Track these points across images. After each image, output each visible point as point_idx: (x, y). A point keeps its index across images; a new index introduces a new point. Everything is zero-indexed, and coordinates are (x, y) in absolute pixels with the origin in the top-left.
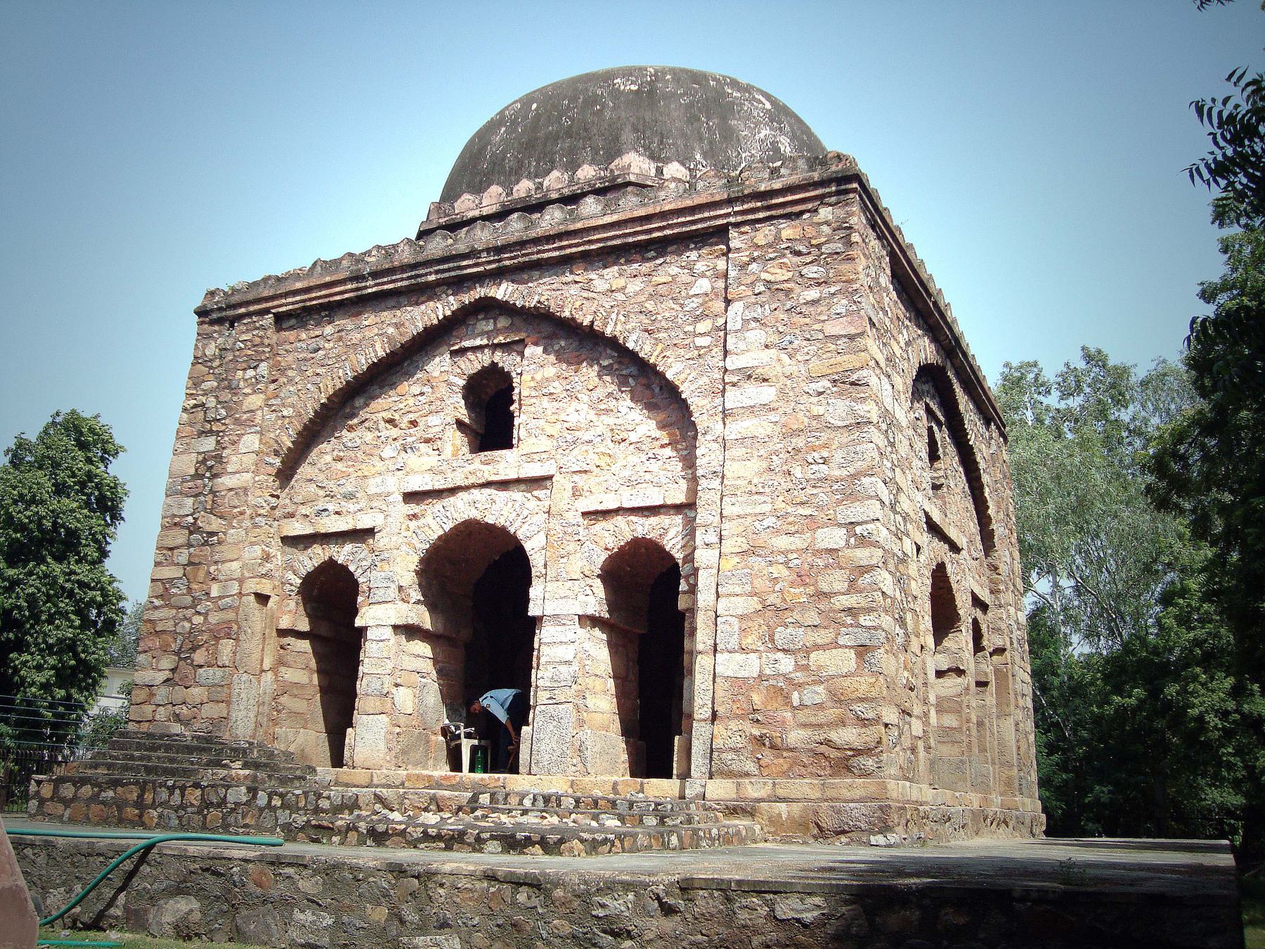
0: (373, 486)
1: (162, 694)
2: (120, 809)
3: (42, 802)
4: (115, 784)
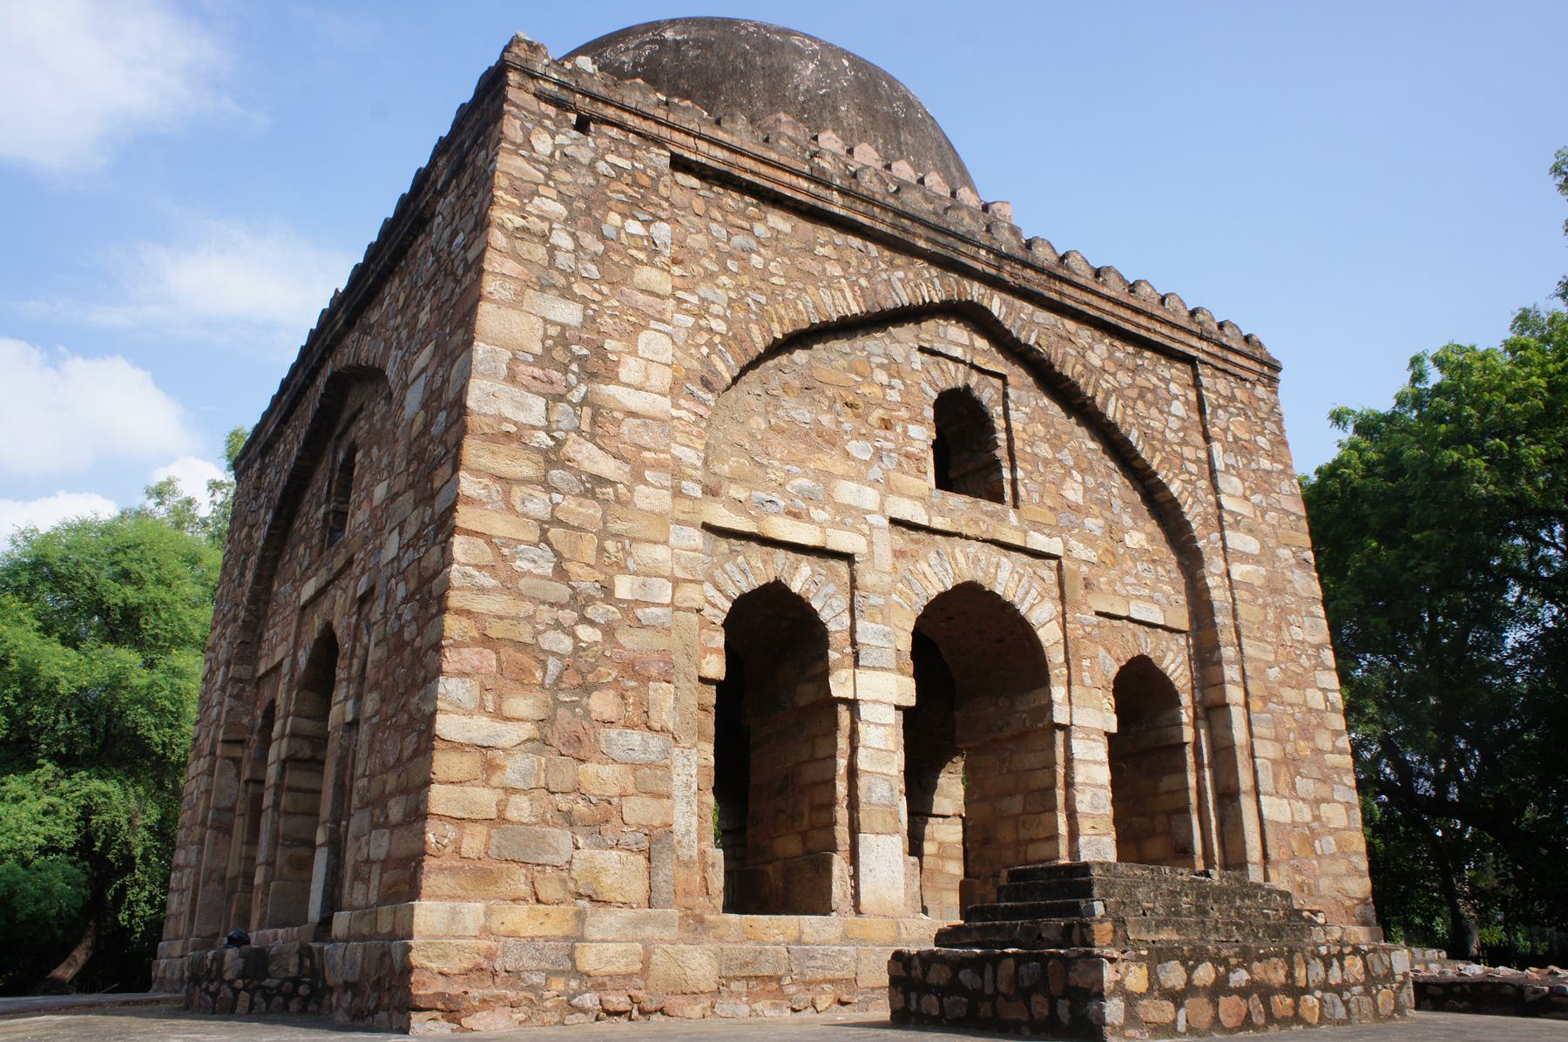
0: (847, 492)
1: (516, 769)
2: (1265, 999)
3: (1131, 999)
4: (1247, 958)
